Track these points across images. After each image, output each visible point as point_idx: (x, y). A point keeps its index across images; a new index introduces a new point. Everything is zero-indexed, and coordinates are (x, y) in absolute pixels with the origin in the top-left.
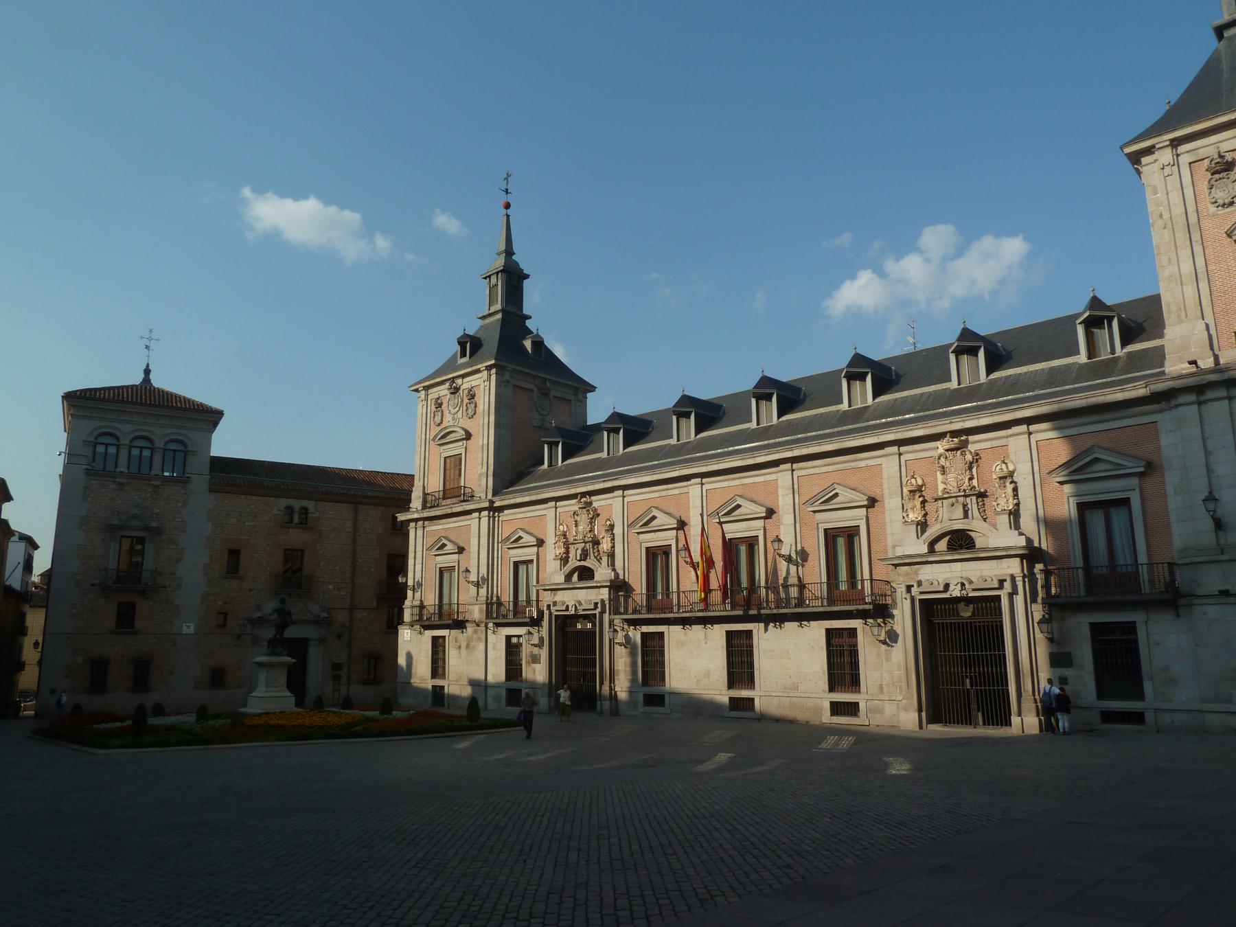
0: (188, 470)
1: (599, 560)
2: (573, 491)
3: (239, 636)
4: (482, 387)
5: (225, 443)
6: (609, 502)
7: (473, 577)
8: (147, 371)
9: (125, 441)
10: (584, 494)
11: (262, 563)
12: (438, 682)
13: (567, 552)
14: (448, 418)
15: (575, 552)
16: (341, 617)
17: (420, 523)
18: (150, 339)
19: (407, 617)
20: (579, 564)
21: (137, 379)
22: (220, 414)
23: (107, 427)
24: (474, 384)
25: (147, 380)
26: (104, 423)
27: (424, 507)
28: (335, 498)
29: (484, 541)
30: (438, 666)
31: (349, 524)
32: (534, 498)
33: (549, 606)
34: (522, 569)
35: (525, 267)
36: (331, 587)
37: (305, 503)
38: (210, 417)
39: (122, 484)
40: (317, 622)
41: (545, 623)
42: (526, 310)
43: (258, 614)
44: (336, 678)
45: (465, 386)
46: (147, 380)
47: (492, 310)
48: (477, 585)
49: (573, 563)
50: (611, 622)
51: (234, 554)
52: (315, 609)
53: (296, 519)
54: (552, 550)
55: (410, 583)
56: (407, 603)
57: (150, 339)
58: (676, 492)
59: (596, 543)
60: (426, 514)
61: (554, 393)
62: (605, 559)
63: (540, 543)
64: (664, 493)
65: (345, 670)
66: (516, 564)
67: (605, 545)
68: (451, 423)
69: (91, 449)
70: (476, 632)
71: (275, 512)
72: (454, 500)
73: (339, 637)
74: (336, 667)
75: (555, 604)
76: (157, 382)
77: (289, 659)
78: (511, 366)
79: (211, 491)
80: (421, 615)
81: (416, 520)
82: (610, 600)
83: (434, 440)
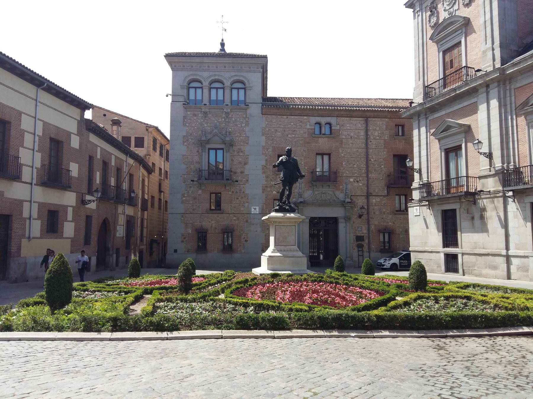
0: (248, 101)
7: (485, 149)
8: (223, 45)
9: (206, 83)
12: (451, 250)
16: (361, 201)
17: (422, 116)
18: (222, 22)
19: (416, 195)
21: (216, 49)
22: (265, 57)
25: (223, 49)
26: (191, 73)
31: (362, 133)
36: (352, 180)
37: (328, 119)
39: (205, 113)
44: (360, 246)
46: (223, 49)
55: (416, 166)
56: (415, 185)
57: (222, 22)
65: (367, 241)
68: (447, 16)
69: (185, 91)
71: (308, 127)
74: (359, 239)
76: (229, 50)
80: (429, 193)
83: (431, 39)
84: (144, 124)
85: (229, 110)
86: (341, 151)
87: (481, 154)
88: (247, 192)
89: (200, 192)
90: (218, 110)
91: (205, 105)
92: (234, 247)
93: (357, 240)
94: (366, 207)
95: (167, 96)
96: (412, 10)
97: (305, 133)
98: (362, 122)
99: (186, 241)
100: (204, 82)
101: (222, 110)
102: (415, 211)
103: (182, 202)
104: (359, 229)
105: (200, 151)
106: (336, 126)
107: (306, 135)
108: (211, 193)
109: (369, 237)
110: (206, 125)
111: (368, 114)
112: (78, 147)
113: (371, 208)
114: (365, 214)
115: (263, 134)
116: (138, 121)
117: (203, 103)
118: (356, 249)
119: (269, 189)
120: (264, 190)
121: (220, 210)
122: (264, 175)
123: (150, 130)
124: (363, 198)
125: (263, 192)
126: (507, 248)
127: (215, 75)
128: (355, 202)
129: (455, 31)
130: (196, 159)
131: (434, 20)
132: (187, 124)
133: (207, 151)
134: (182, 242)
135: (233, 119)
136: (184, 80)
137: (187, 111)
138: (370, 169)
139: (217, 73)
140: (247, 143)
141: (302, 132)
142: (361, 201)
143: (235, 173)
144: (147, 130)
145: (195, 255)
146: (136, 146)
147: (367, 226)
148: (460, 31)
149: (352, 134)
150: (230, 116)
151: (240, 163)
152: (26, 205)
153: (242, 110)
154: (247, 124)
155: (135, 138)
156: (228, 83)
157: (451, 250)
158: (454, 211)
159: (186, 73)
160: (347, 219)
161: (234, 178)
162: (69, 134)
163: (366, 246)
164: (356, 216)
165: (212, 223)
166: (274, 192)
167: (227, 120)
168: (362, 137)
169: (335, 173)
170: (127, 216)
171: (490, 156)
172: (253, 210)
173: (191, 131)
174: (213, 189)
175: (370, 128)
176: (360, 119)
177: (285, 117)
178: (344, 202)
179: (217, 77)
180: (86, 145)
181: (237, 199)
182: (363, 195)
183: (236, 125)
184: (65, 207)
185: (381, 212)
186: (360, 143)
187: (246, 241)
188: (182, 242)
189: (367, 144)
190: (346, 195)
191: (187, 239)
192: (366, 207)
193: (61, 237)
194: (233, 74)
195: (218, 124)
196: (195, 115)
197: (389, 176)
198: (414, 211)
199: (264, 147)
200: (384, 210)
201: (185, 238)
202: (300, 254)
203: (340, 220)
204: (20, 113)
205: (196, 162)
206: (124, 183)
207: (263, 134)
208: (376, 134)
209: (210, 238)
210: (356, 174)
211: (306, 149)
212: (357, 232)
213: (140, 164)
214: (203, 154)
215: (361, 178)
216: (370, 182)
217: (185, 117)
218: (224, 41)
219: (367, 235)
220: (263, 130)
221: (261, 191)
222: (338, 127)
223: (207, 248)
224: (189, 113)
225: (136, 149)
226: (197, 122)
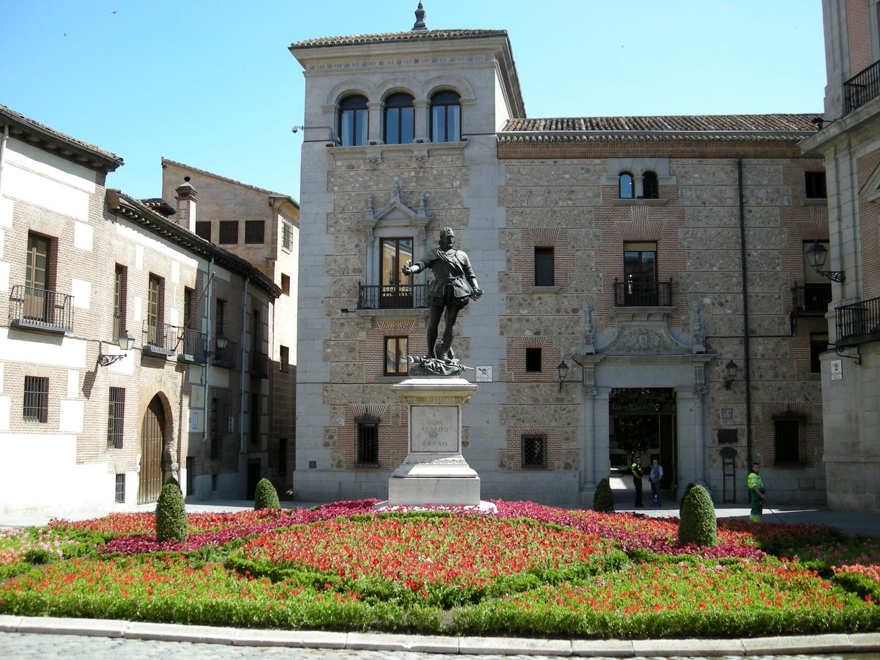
0: (464, 131)
8: (420, 15)
21: (406, 25)
22: (503, 34)
31: (731, 193)
36: (707, 301)
37: (650, 164)
43: (591, 349)
44: (728, 454)
46: (419, 26)
51: (544, 253)
56: (831, 307)
60: (850, 122)
65: (743, 441)
71: (604, 181)
73: (728, 385)
74: (727, 436)
76: (432, 24)
79: (499, 158)
84: (265, 192)
85: (425, 153)
86: (680, 235)
90: (402, 154)
91: (373, 144)
93: (721, 441)
94: (741, 364)
95: (295, 132)
97: (597, 196)
98: (728, 168)
99: (334, 443)
102: (833, 369)
103: (326, 359)
104: (727, 415)
105: (363, 244)
106: (667, 179)
107: (600, 201)
108: (386, 339)
110: (375, 188)
111: (740, 149)
112: (89, 248)
113: (754, 365)
114: (741, 379)
115: (500, 204)
116: (251, 188)
117: (370, 141)
118: (719, 460)
119: (515, 325)
120: (501, 327)
122: (504, 295)
124: (736, 341)
125: (502, 333)
127: (395, 80)
128: (714, 352)
130: (354, 262)
132: (336, 188)
133: (377, 243)
134: (327, 445)
135: (435, 172)
136: (331, 95)
137: (335, 161)
138: (749, 275)
140: (466, 224)
141: (590, 194)
144: (271, 205)
145: (353, 474)
146: (248, 240)
149: (705, 196)
150: (428, 165)
153: (452, 152)
154: (465, 182)
155: (247, 223)
159: (335, 80)
162: (70, 223)
163: (742, 455)
164: (718, 385)
166: (528, 333)
167: (421, 175)
168: (730, 202)
169: (669, 285)
170: (212, 388)
172: (479, 373)
173: (342, 203)
175: (748, 181)
176: (725, 161)
177: (550, 162)
178: (690, 351)
180: (110, 244)
182: (734, 334)
183: (440, 184)
184: (63, 371)
185: (776, 375)
186: (727, 215)
188: (327, 445)
189: (742, 218)
191: (335, 438)
194: (433, 74)
195: (401, 183)
196: (351, 167)
199: (502, 231)
200: (784, 369)
201: (331, 437)
203: (680, 395)
205: (354, 270)
206: (204, 320)
207: (500, 204)
208: (762, 193)
210: (718, 288)
211: (599, 232)
213: (244, 277)
215: (729, 297)
216: (751, 306)
217: (330, 173)
218: (424, 8)
220: (500, 192)
221: (497, 330)
222: (673, 181)
223: (380, 459)
224: (339, 163)
225: (249, 245)
226: (357, 181)
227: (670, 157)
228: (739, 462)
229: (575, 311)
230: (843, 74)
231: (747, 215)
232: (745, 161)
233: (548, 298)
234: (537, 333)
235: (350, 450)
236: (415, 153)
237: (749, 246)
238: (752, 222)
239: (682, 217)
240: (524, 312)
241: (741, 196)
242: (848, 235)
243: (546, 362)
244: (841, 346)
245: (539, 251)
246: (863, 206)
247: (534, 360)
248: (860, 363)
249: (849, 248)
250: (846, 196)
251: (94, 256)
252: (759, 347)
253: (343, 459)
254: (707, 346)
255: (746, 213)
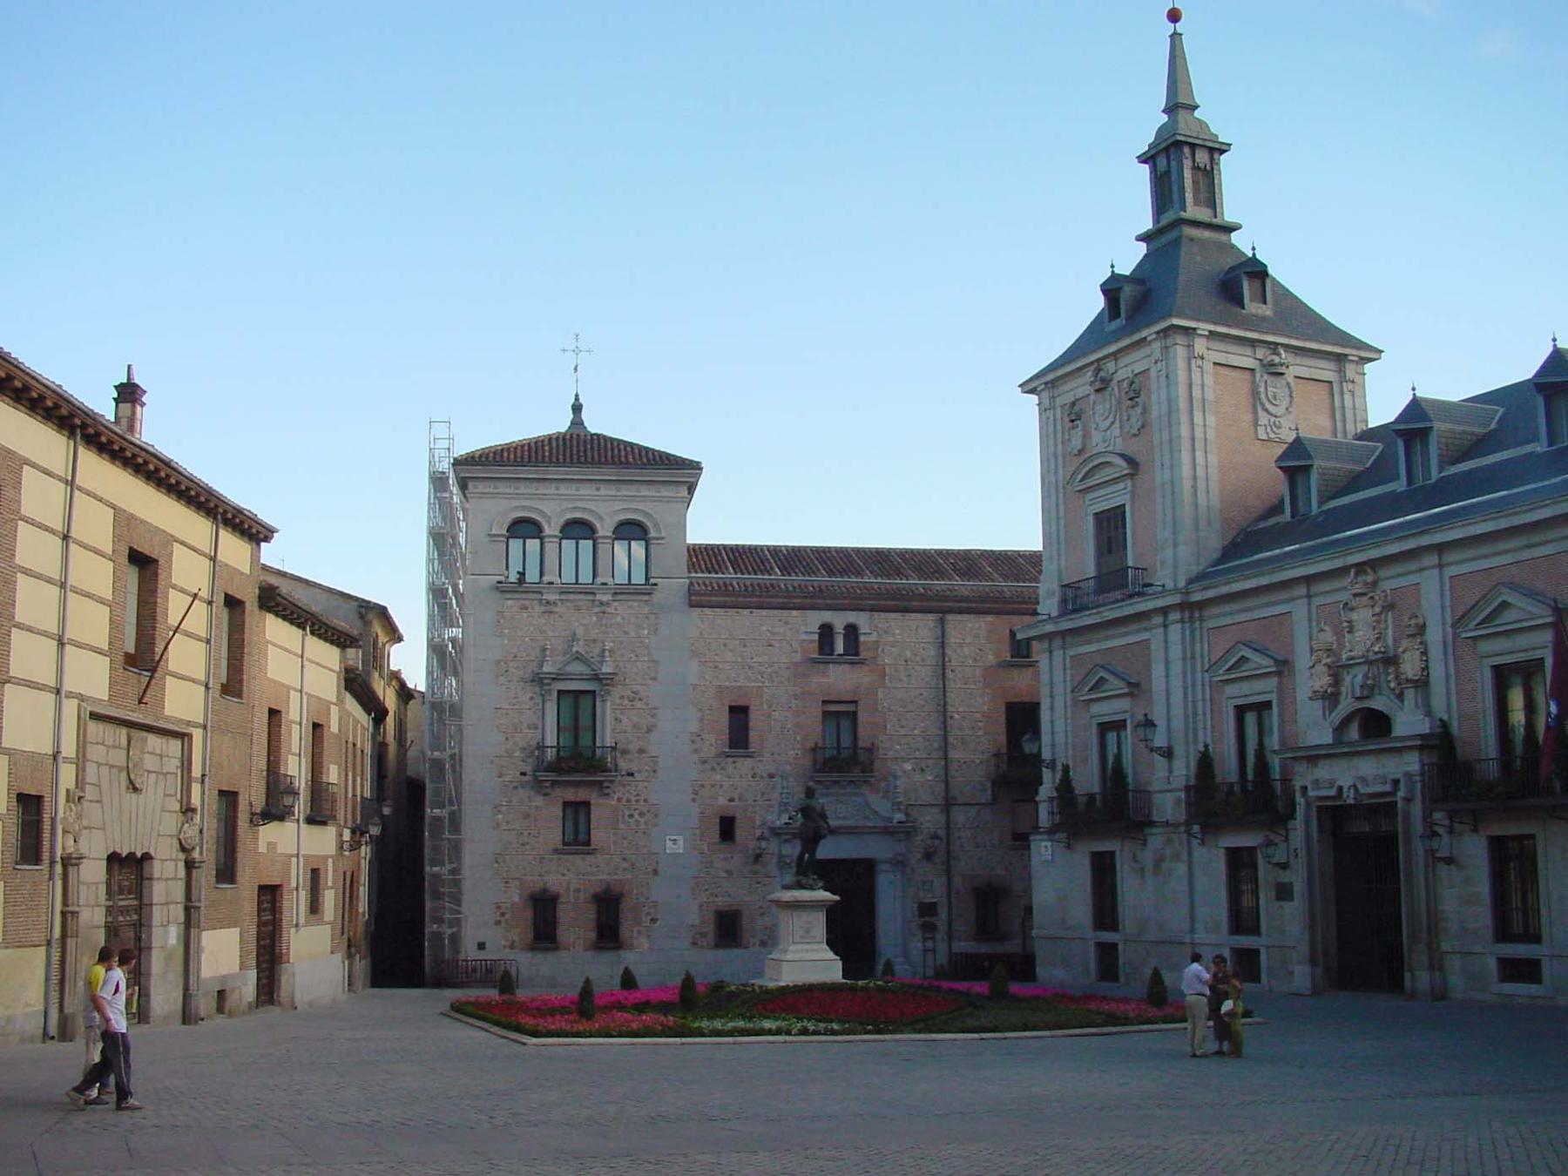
0: (654, 571)
1: (1400, 696)
2: (1338, 563)
3: (758, 857)
4: (1153, 373)
5: (712, 520)
6: (1413, 579)
8: (577, 408)
10: (1360, 568)
11: (786, 731)
12: (1108, 936)
13: (1337, 681)
14: (1096, 438)
15: (1353, 681)
17: (1057, 642)
18: (577, 351)
20: (1359, 705)
22: (695, 467)
23: (524, 508)
24: (1138, 368)
25: (577, 422)
27: (1064, 613)
28: (902, 604)
29: (1177, 667)
30: (1105, 909)
32: (1264, 581)
33: (1304, 789)
34: (1251, 718)
35: (1221, 131)
36: (908, 766)
38: (680, 474)
40: (888, 831)
41: (1298, 824)
42: (1229, 216)
44: (929, 928)
45: (1121, 375)
46: (577, 422)
47: (1165, 220)
48: (1168, 753)
49: (1346, 705)
50: (1427, 815)
51: (739, 714)
52: (881, 805)
53: (840, 647)
54: (1309, 679)
55: (1046, 754)
56: (1046, 790)
58: (1548, 550)
59: (1391, 661)
60: (1066, 625)
61: (1291, 372)
62: (1410, 694)
63: (1283, 667)
64: (1526, 555)
65: (944, 916)
66: (1241, 711)
67: (1410, 667)
70: (1169, 842)
72: (1118, 594)
73: (928, 856)
74: (927, 909)
75: (1316, 783)
77: (827, 895)
78: (1204, 327)
81: (1050, 636)
82: (1422, 774)
84: (356, 599)
86: (880, 695)
87: (1152, 750)
88: (651, 801)
89: (539, 801)
92: (625, 933)
93: (921, 916)
94: (941, 833)
96: (1034, 398)
98: (932, 624)
100: (546, 527)
101: (590, 597)
109: (950, 903)
118: (919, 934)
121: (588, 843)
122: (696, 757)
123: (371, 616)
124: (936, 810)
126: (1192, 931)
129: (1115, 481)
131: (1077, 442)
134: (498, 923)
138: (951, 739)
139: (579, 504)
140: (654, 679)
142: (930, 820)
143: (624, 752)
144: (362, 616)
145: (529, 955)
147: (944, 879)
148: (1121, 485)
151: (636, 726)
152: (294, 860)
156: (604, 529)
157: (1108, 936)
158: (1112, 854)
159: (504, 504)
160: (900, 864)
161: (624, 765)
164: (918, 856)
165: (573, 879)
166: (722, 801)
171: (1168, 753)
172: (669, 844)
174: (570, 794)
177: (746, 612)
178: (890, 820)
179: (578, 515)
181: (631, 816)
183: (626, 633)
187: (653, 920)
190: (897, 806)
192: (941, 833)
193: (321, 922)
197: (997, 755)
198: (1042, 849)
199: (695, 686)
201: (503, 914)
202: (831, 955)
204: (289, 688)
209: (565, 913)
212: (921, 894)
214: (548, 704)
219: (945, 900)
222: (873, 638)
227: (873, 610)
228: (938, 937)
229: (771, 776)
230: (1060, 572)
231: (949, 675)
232: (949, 617)
233: (745, 765)
234: (732, 800)
235: (522, 930)
236: (598, 597)
237: (950, 708)
238: (955, 685)
239: (883, 675)
240: (718, 777)
241: (944, 655)
242: (1060, 725)
243: (740, 832)
244: (1051, 831)
245: (732, 709)
246: (1075, 702)
247: (727, 828)
248: (1069, 847)
249: (1060, 738)
250: (1059, 690)
251: (338, 737)
252: (960, 816)
253: (516, 938)
254: (907, 814)
255: (948, 672)
